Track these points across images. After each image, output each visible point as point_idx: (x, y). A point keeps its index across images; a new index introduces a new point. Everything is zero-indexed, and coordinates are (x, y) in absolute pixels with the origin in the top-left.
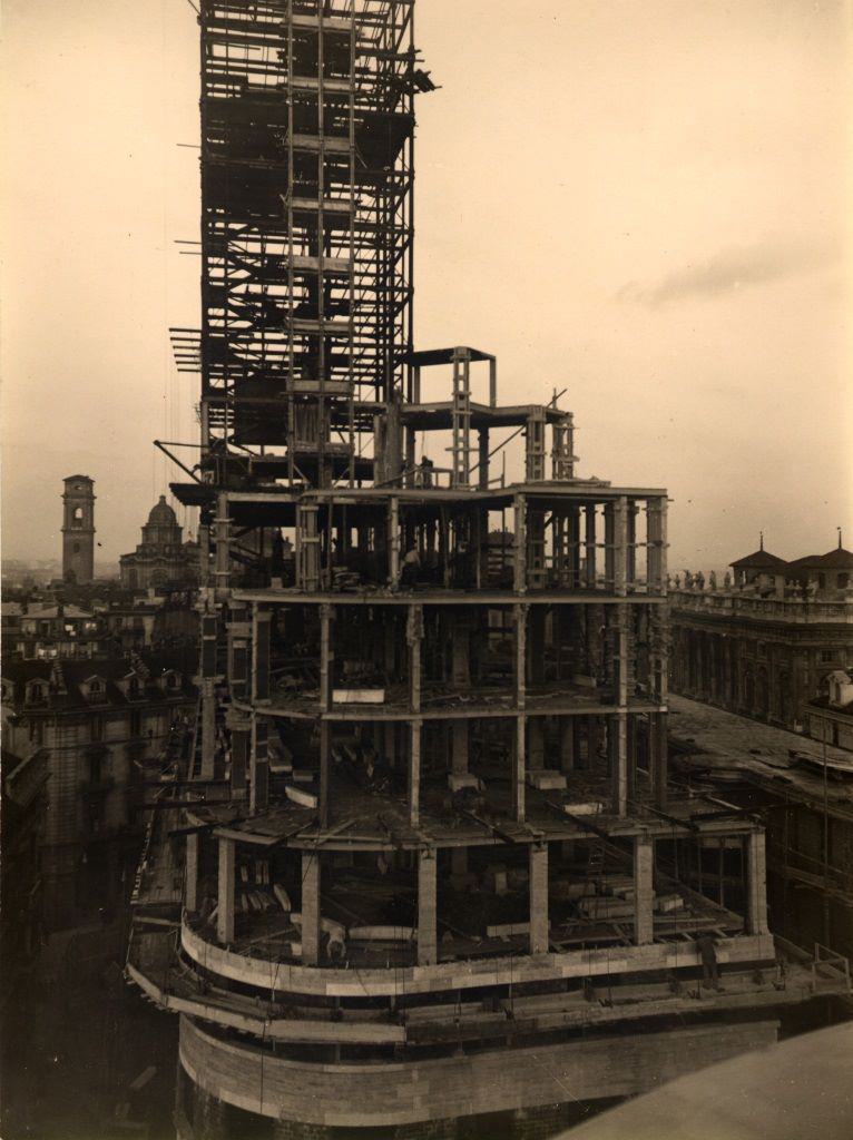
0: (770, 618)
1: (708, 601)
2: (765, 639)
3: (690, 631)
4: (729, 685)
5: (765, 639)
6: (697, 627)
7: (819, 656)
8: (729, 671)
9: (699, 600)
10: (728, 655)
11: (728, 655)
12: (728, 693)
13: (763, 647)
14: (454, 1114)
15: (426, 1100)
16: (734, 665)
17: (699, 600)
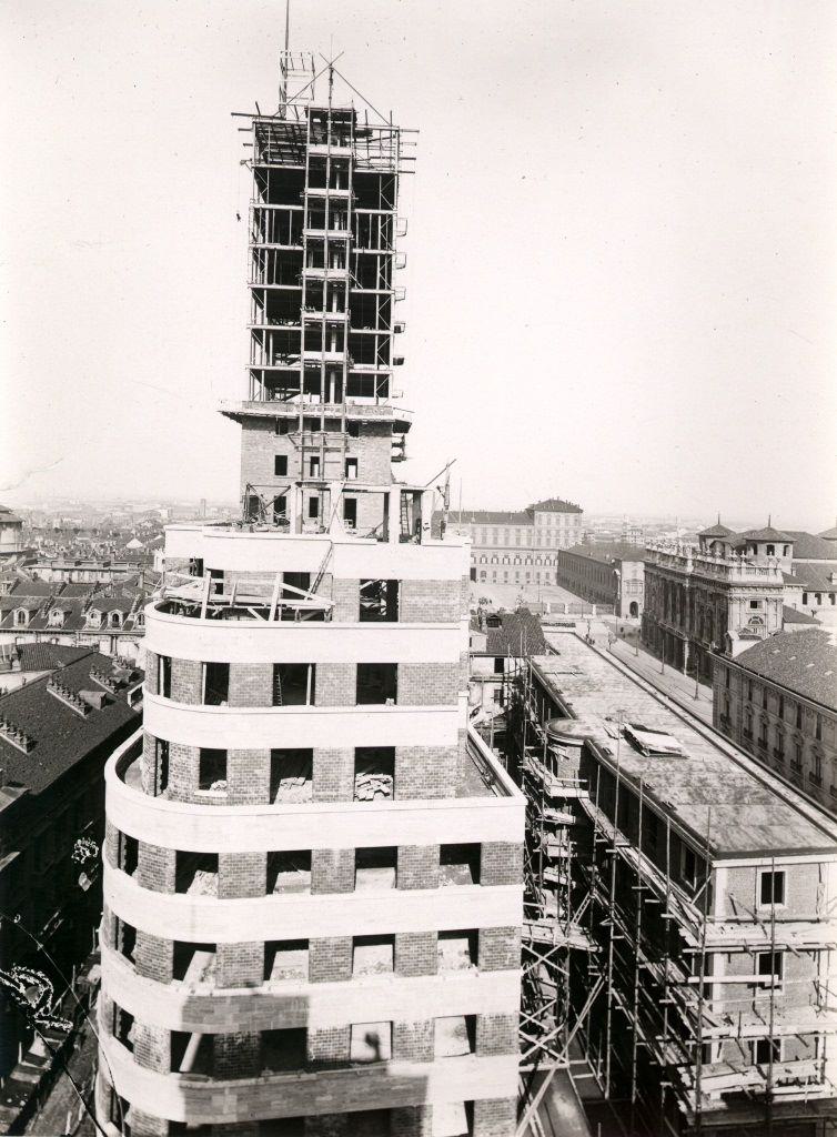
0: (716, 577)
1: (677, 560)
2: (711, 590)
3: (664, 579)
4: (688, 620)
5: (711, 590)
6: (669, 578)
7: (748, 604)
8: (688, 611)
9: (671, 560)
10: (688, 599)
11: (688, 599)
12: (687, 626)
13: (711, 595)
14: (255, 1030)
15: (236, 1018)
16: (692, 606)
17: (671, 560)
